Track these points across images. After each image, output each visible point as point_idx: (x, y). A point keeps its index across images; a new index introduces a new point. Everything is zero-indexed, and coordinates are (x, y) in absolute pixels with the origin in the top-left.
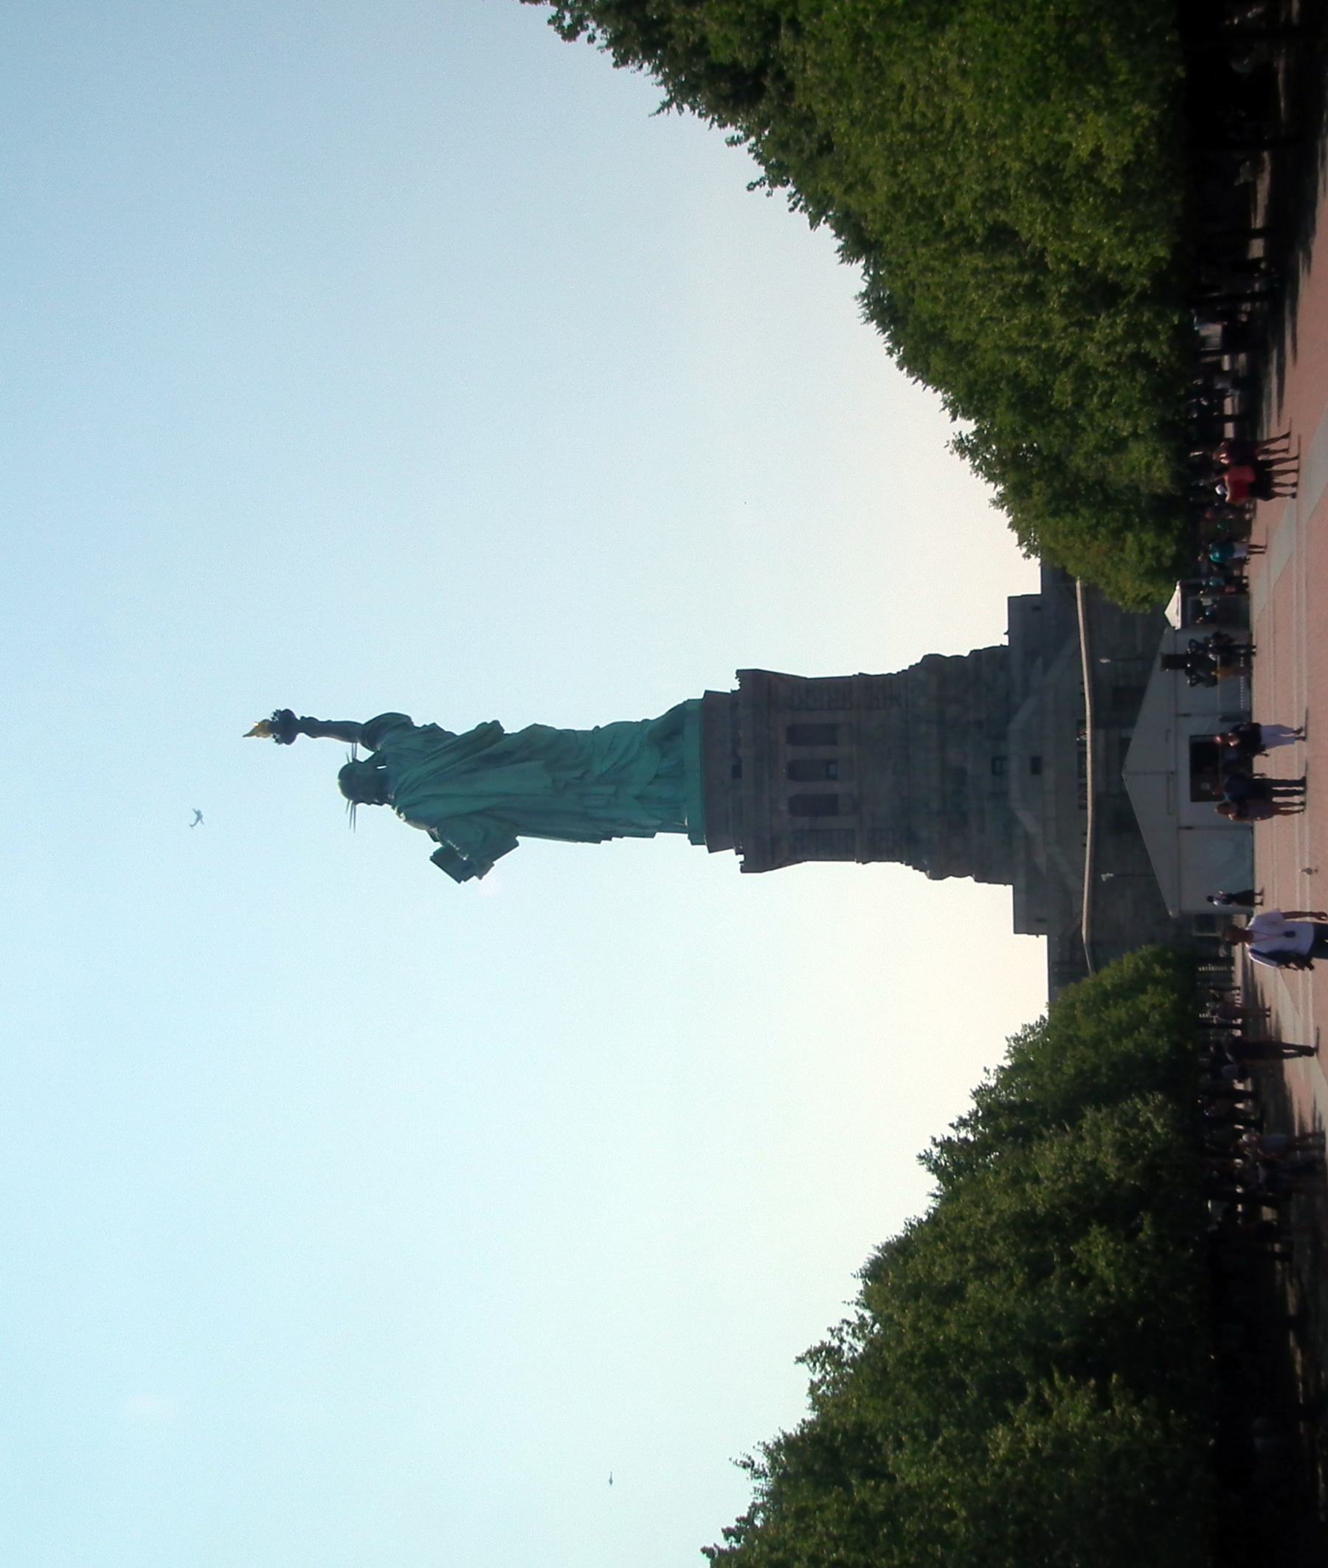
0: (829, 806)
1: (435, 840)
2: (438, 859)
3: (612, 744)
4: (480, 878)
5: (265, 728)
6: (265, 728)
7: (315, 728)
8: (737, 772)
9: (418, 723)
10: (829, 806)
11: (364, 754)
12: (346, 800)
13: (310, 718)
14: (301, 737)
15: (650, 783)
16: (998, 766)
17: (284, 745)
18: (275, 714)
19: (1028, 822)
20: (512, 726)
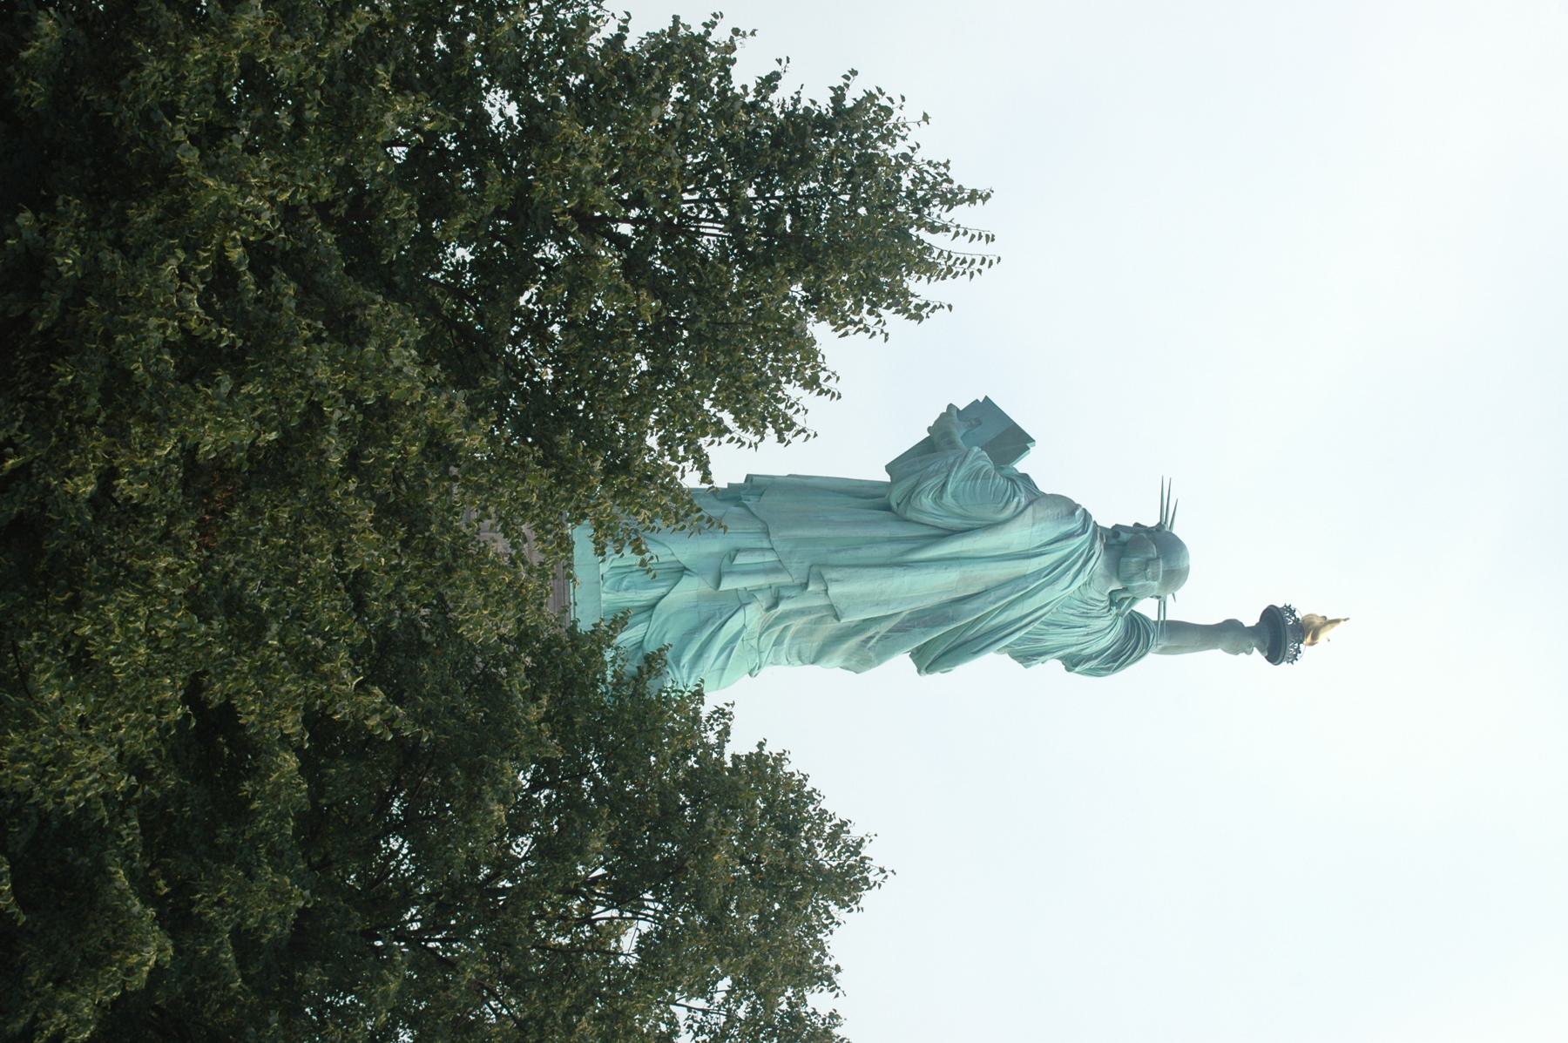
1: (1025, 477)
4: (950, 406)
5: (1307, 630)
6: (1307, 630)
7: (1227, 634)
9: (1054, 666)
11: (1147, 608)
12: (1175, 531)
13: (1236, 653)
14: (1251, 619)
17: (1280, 605)
18: (1295, 658)
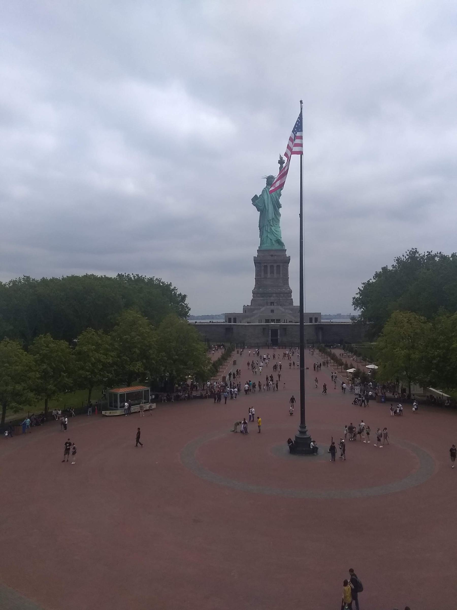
0: (266, 272)
2: (256, 196)
3: (278, 231)
8: (272, 256)
10: (266, 272)
15: (270, 238)
16: (272, 303)
19: (263, 309)
20: (281, 210)
